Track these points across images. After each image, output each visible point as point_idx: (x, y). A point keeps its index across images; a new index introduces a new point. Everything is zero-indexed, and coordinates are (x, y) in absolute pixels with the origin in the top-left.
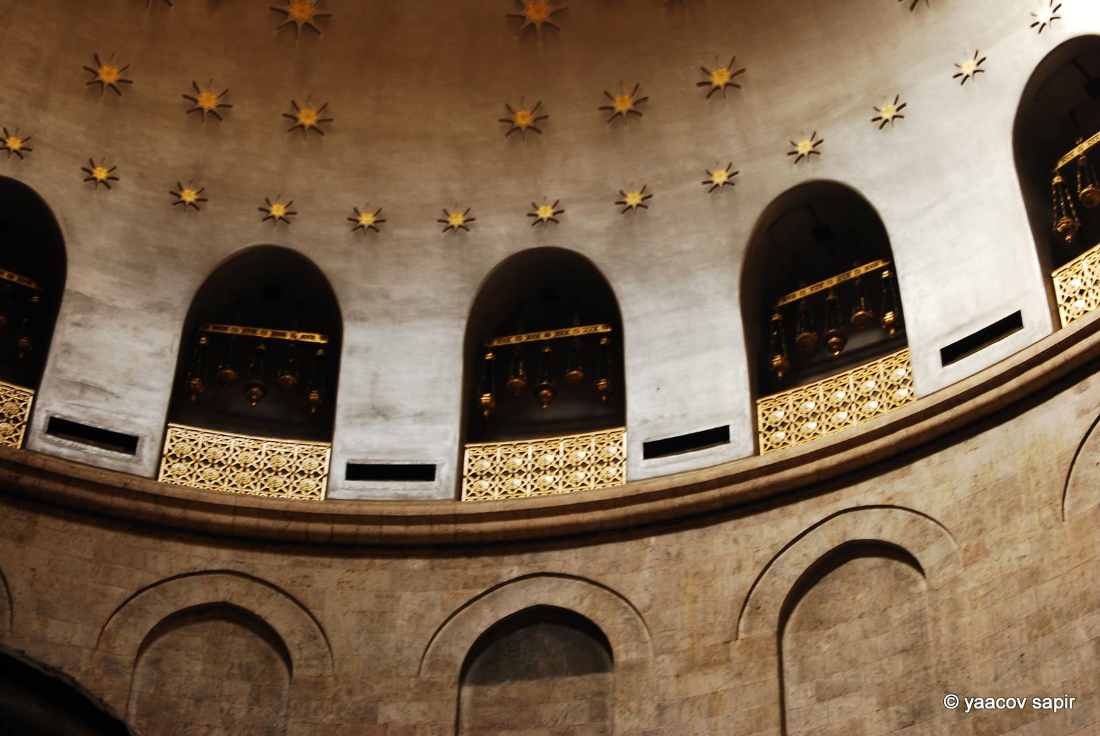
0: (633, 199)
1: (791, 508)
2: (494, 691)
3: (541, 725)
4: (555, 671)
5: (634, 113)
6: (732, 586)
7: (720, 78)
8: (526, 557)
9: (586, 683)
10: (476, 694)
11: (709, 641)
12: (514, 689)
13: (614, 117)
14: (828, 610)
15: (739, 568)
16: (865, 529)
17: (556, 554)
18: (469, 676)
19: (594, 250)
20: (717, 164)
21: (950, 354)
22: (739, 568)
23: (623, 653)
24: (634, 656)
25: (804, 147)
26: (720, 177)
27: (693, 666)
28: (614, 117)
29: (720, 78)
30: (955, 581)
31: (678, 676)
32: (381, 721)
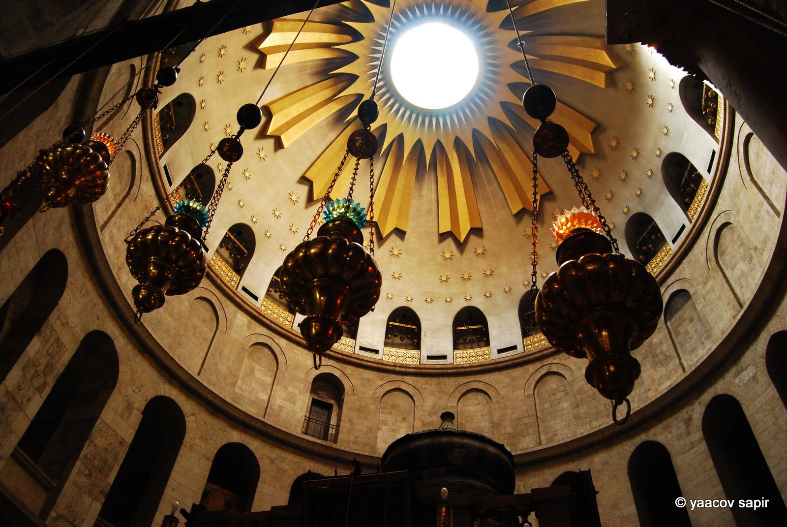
0: (638, 193)
1: (704, 231)
2: (673, 319)
3: (686, 320)
4: (682, 305)
5: (626, 176)
6: (702, 259)
7: (635, 154)
8: (664, 285)
9: (689, 303)
10: (671, 323)
11: (705, 275)
12: (677, 316)
13: (624, 180)
14: (724, 248)
15: (702, 253)
16: (718, 225)
17: (669, 280)
18: (667, 320)
19: (640, 210)
20: (647, 171)
21: (709, 171)
22: (702, 253)
23: (691, 291)
24: (694, 290)
25: (658, 153)
26: (649, 173)
27: (705, 283)
28: (624, 180)
29: (635, 154)
30: (738, 221)
31: (703, 288)
32: (654, 343)
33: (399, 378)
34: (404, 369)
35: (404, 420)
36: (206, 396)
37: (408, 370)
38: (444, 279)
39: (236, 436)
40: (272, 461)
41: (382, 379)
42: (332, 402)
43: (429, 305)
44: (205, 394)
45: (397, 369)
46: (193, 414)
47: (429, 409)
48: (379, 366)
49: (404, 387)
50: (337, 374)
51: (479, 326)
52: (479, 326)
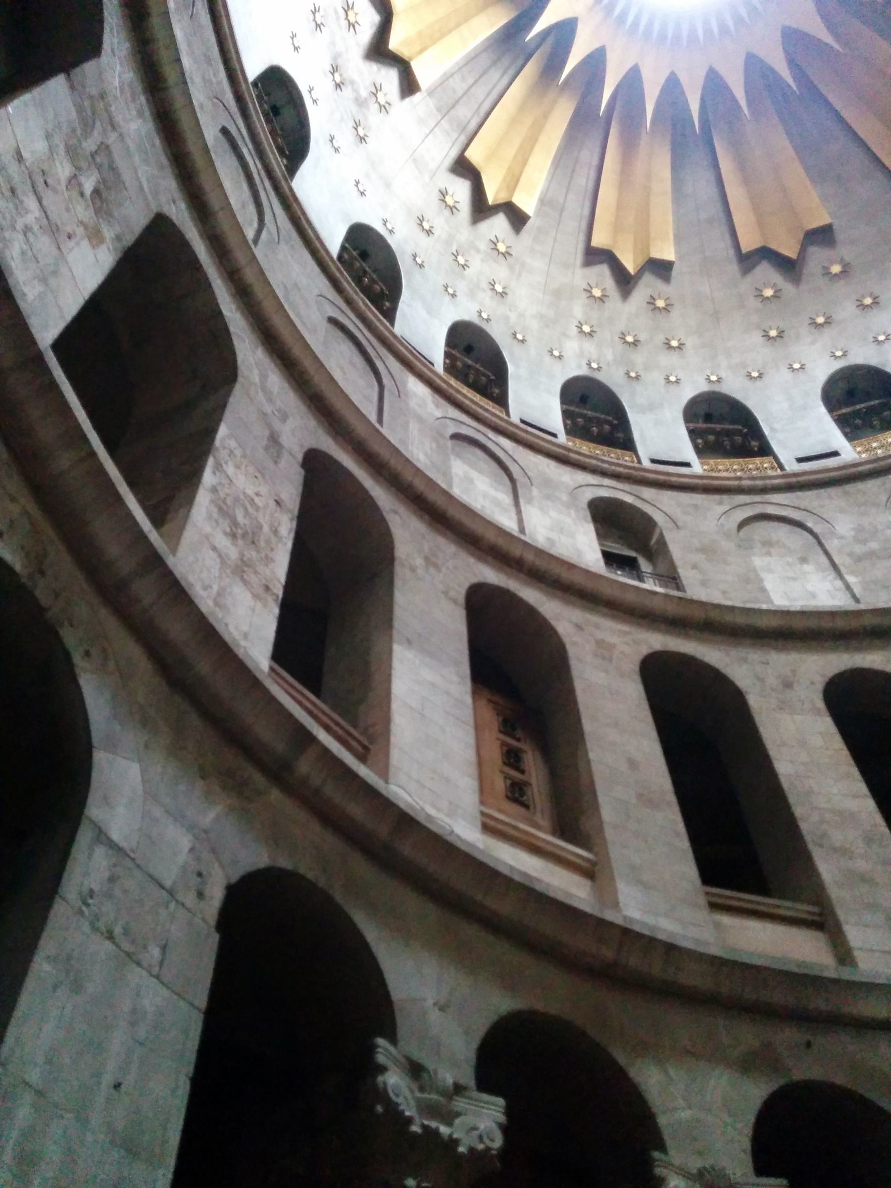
33: (757, 498)
34: (759, 483)
35: (804, 560)
36: (411, 482)
37: (768, 482)
38: (773, 333)
39: (491, 575)
40: (579, 627)
41: (720, 503)
42: (633, 554)
43: (759, 383)
44: (408, 476)
45: (746, 483)
46: (395, 512)
47: (853, 533)
48: (705, 481)
49: (771, 510)
50: (628, 499)
51: (877, 402)
52: (877, 402)
